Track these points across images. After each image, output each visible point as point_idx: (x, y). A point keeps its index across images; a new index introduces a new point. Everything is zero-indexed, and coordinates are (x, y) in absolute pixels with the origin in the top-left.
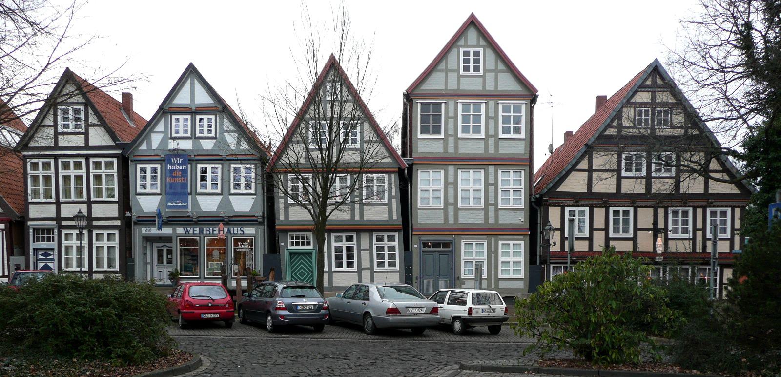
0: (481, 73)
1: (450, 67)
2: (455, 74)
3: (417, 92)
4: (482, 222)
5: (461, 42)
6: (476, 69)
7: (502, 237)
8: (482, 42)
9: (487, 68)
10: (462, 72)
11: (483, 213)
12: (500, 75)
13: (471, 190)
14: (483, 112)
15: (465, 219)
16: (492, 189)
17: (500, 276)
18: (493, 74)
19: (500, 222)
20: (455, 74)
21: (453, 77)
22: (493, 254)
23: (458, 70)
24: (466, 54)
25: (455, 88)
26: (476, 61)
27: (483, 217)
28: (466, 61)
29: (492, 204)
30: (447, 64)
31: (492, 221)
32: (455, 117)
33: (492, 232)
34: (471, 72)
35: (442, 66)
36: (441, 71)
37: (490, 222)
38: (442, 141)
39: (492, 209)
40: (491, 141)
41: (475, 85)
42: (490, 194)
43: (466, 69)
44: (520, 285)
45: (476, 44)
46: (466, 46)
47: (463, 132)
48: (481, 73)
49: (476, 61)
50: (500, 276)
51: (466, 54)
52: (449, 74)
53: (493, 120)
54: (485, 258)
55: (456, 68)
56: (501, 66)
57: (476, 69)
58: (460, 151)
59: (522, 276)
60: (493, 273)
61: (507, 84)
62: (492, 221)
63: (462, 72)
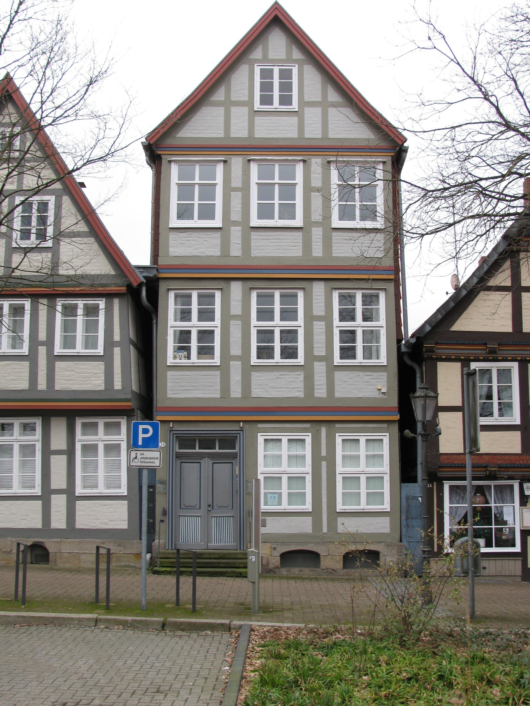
0: (295, 106)
2: (245, 110)
4: (301, 394)
5: (257, 54)
6: (286, 100)
8: (297, 54)
9: (306, 99)
10: (257, 106)
11: (302, 377)
12: (332, 112)
14: (299, 179)
16: (319, 327)
17: (340, 507)
18: (318, 111)
20: (245, 110)
21: (239, 115)
22: (324, 460)
23: (250, 103)
24: (267, 74)
25: (245, 134)
26: (286, 87)
27: (302, 384)
28: (267, 87)
29: (320, 359)
30: (228, 92)
31: (320, 392)
32: (245, 189)
33: (322, 417)
35: (219, 95)
36: (218, 104)
37: (316, 395)
38: (218, 234)
40: (317, 233)
41: (283, 129)
42: (316, 338)
43: (266, 100)
44: (383, 526)
45: (284, 57)
46: (265, 59)
47: (260, 216)
48: (295, 106)
49: (286, 87)
50: (340, 507)
51: (267, 74)
52: (233, 109)
54: (308, 468)
55: (246, 98)
56: (333, 96)
57: (286, 100)
58: (254, 253)
60: (324, 500)
61: (345, 127)
62: (320, 392)
63: (257, 106)
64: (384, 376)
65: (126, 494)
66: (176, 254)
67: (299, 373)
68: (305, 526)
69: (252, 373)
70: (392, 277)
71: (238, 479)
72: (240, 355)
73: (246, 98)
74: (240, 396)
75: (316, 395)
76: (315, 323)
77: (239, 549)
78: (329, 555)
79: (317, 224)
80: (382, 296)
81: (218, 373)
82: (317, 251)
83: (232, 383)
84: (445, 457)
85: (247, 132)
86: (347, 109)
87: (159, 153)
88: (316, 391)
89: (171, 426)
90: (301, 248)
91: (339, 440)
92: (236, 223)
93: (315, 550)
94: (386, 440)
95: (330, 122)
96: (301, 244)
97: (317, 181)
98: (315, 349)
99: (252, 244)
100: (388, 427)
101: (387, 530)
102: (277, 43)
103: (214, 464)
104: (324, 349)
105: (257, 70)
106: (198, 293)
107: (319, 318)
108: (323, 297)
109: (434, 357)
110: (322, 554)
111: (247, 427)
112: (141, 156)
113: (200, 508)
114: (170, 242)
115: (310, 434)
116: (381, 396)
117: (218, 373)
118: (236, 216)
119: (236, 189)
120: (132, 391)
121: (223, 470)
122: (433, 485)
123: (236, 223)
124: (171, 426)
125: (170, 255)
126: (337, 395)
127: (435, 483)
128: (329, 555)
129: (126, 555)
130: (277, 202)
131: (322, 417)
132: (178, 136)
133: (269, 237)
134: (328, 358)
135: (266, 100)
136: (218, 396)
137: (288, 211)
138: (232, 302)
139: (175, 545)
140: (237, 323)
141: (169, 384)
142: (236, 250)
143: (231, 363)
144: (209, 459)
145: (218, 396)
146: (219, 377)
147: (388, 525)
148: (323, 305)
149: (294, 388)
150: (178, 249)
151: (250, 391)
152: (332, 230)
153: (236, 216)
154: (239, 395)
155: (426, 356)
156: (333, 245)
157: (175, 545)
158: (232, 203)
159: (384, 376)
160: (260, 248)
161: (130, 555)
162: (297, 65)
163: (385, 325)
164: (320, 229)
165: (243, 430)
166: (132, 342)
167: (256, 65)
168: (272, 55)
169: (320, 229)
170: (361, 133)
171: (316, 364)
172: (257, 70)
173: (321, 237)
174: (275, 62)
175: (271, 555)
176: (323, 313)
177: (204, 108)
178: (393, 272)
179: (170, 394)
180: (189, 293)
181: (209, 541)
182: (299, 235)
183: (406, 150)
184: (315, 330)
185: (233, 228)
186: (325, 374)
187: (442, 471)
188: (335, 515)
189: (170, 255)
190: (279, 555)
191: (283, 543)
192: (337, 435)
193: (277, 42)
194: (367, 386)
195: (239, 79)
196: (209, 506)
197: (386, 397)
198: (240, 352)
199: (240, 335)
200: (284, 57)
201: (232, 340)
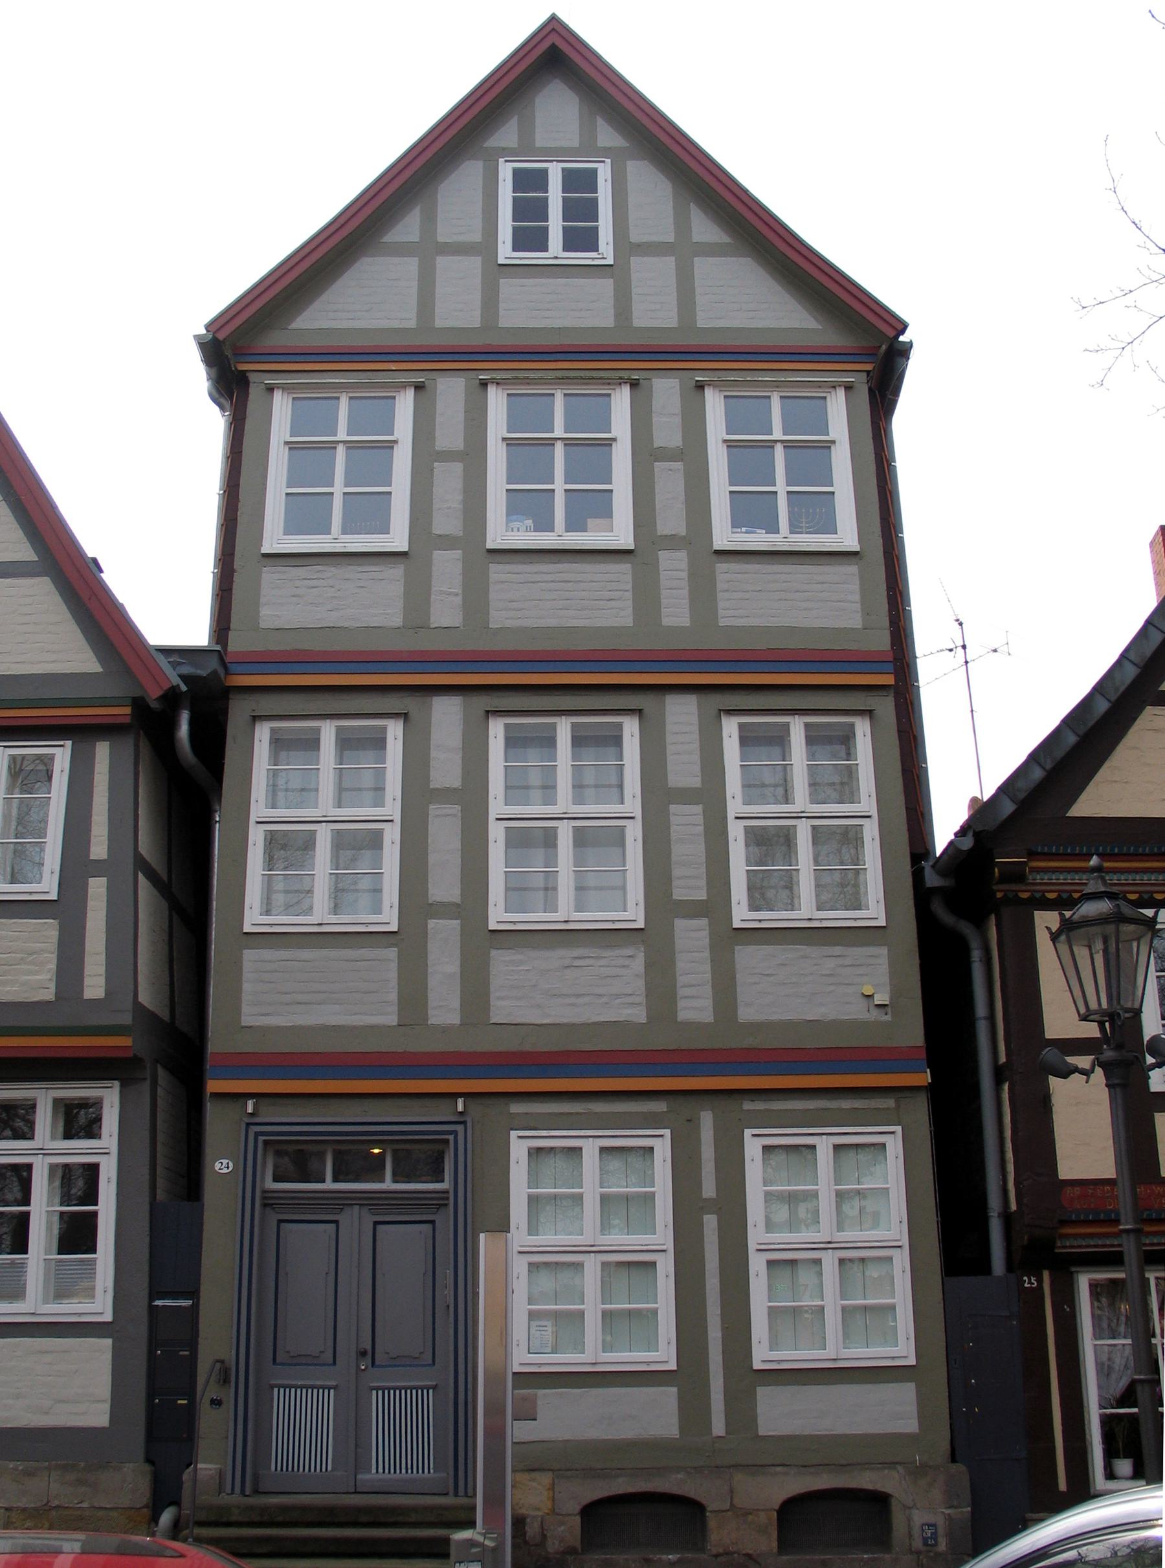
0: (606, 251)
1: (444, 235)
3: (276, 339)
5: (507, 135)
6: (581, 238)
7: (759, 1105)
8: (607, 136)
9: (635, 236)
10: (505, 252)
11: (638, 965)
12: (703, 267)
13: (565, 834)
15: (534, 998)
16: (686, 820)
17: (762, 1355)
22: (709, 1215)
24: (530, 182)
26: (581, 210)
28: (530, 212)
30: (430, 220)
32: (473, 456)
33: (703, 1081)
37: (683, 1015)
38: (396, 572)
39: (692, 938)
40: (673, 567)
42: (678, 851)
43: (530, 237)
44: (896, 1411)
45: (575, 143)
46: (526, 147)
48: (606, 251)
49: (581, 210)
50: (762, 1355)
51: (530, 182)
53: (678, 465)
54: (662, 1235)
55: (477, 237)
56: (705, 229)
57: (581, 238)
58: (498, 618)
59: (901, 1349)
61: (741, 300)
63: (505, 252)
64: (879, 957)
65: (108, 1317)
66: (278, 624)
67: (628, 952)
68: (656, 1416)
69: (493, 953)
71: (450, 1272)
72: (458, 900)
73: (477, 237)
74: (457, 1021)
75: (683, 1015)
76: (673, 808)
77: (451, 1492)
79: (672, 542)
80: (862, 729)
81: (392, 953)
82: (676, 611)
83: (433, 982)
84: (1077, 1190)
85: (478, 313)
86: (743, 260)
88: (681, 1004)
89: (250, 1110)
90: (630, 603)
91: (753, 1147)
92: (447, 542)
93: (692, 1494)
94: (894, 1145)
95: (698, 291)
96: (629, 595)
97: (668, 432)
98: (675, 883)
99: (492, 596)
100: (898, 1107)
101: (911, 1426)
102: (557, 111)
103: (380, 1228)
104: (703, 882)
105: (506, 171)
106: (339, 730)
107: (686, 796)
108: (696, 736)
109: (1025, 895)
110: (711, 1506)
111: (477, 1110)
112: (196, 376)
113: (334, 1363)
114: (263, 592)
116: (875, 1015)
117: (392, 953)
118: (447, 522)
119: (448, 456)
120: (137, 1006)
121: (404, 1244)
122: (1040, 1281)
123: (447, 542)
124: (250, 1110)
125: (263, 625)
126: (746, 1014)
127: (1046, 1275)
129: (100, 1513)
131: (703, 1081)
132: (294, 325)
133: (538, 578)
134: (715, 905)
135: (530, 237)
136: (392, 1020)
138: (434, 753)
139: (256, 1478)
140: (450, 812)
141: (247, 987)
142: (446, 611)
143: (432, 923)
144: (365, 1210)
145: (392, 1020)
146: (394, 966)
147: (912, 1408)
148: (696, 758)
149: (617, 996)
150: (285, 609)
151: (486, 1008)
152: (714, 557)
153: (447, 522)
154: (455, 1019)
155: (999, 895)
156: (720, 595)
157: (256, 1478)
158: (437, 491)
159: (879, 957)
160: (515, 605)
161: (114, 1514)
163: (874, 812)
164: (682, 555)
165: (464, 1123)
166: (141, 864)
167: (501, 160)
168: (541, 140)
169: (682, 555)
170: (779, 314)
171: (680, 924)
172: (506, 171)
173: (685, 575)
175: (553, 1511)
176: (695, 782)
178: (891, 667)
179: (250, 1017)
180: (311, 728)
181: (360, 1463)
182: (623, 570)
183: (904, 351)
184: (673, 828)
186: (707, 954)
187: (1067, 1236)
189: (263, 625)
190: (578, 1509)
191: (591, 1473)
194: (832, 988)
196: (364, 1354)
197: (888, 1018)
198: (458, 892)
199: (456, 844)
201: (432, 858)
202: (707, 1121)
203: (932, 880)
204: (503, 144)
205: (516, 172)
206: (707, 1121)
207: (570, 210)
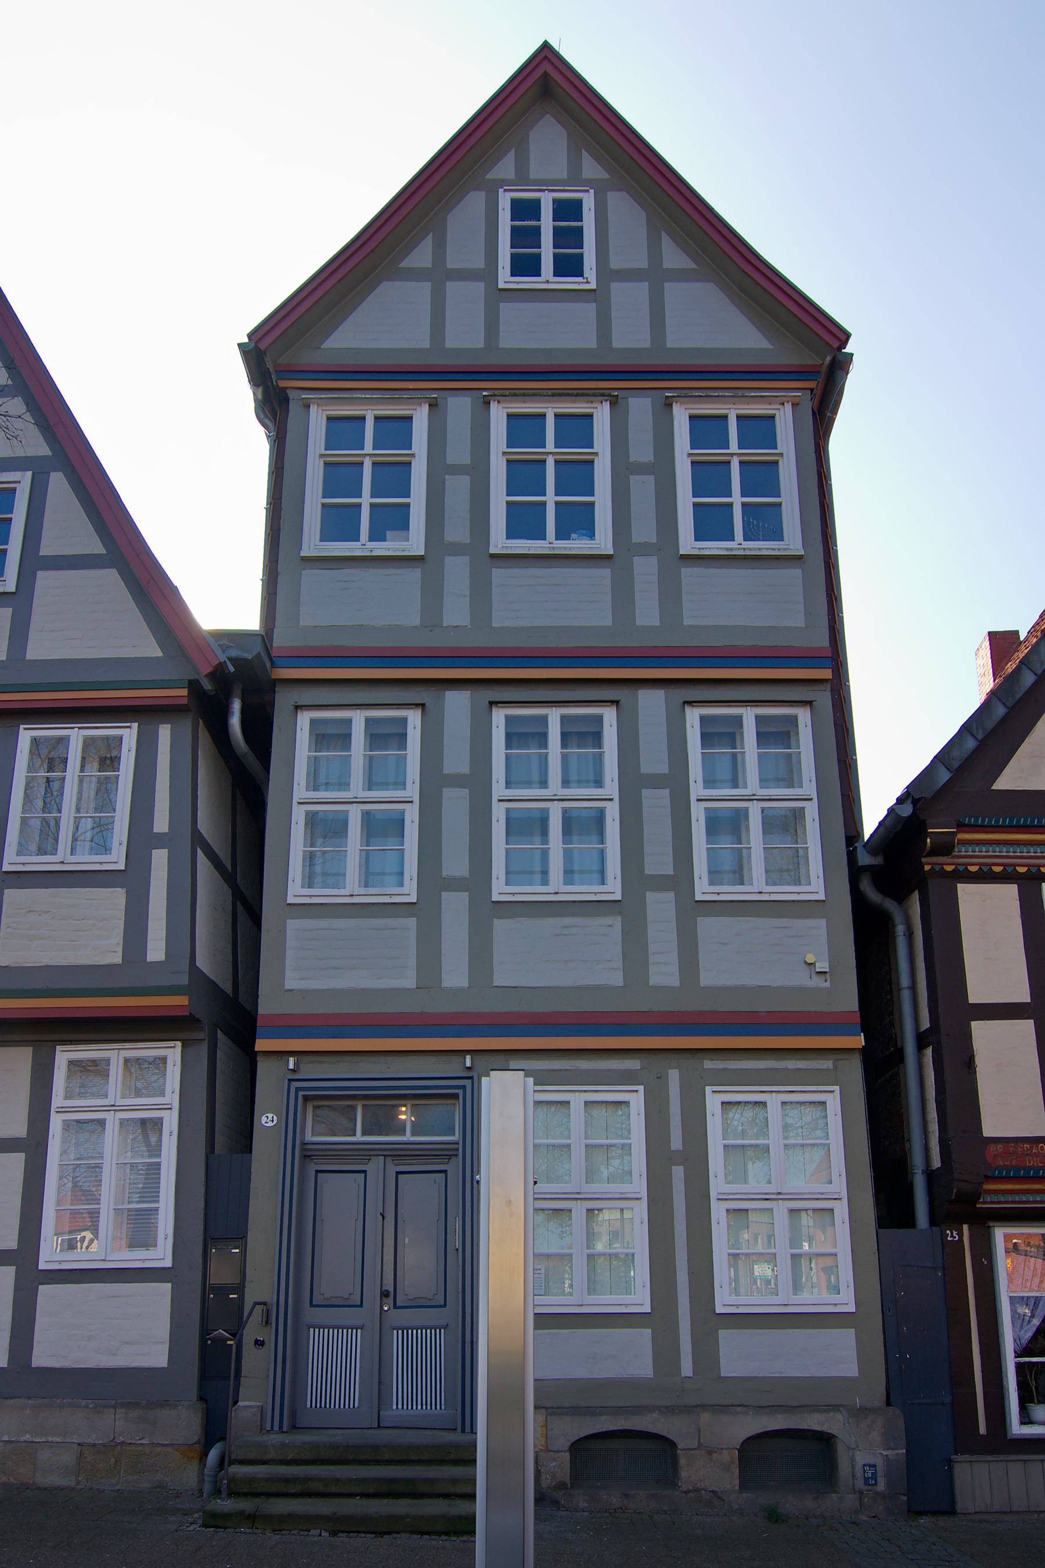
2: (478, 288)
8: (591, 169)
9: (615, 264)
10: (505, 278)
18: (641, 290)
19: (707, 979)
20: (478, 288)
21: (465, 302)
24: (525, 210)
25: (478, 341)
26: (568, 237)
28: (525, 237)
34: (547, 277)
36: (416, 275)
43: (525, 265)
45: (564, 176)
52: (451, 286)
55: (480, 263)
57: (568, 265)
70: (827, 674)
73: (480, 263)
78: (700, 1446)
82: (647, 613)
87: (283, 384)
88: (653, 969)
91: (713, 1101)
92: (457, 549)
115: (641, 1088)
128: (700, 1446)
130: (550, 498)
137: (577, 520)
162: (592, 191)
169: (654, 560)
174: (545, 185)
177: (385, 285)
182: (603, 575)
185: (449, 560)
188: (711, 1322)
192: (708, 1089)
193: (548, 145)
195: (466, 216)
197: (827, 984)
200: (564, 176)
202: (674, 1076)
203: (864, 859)
204: (501, 177)
205: (514, 202)
206: (674, 1076)
207: (561, 237)
